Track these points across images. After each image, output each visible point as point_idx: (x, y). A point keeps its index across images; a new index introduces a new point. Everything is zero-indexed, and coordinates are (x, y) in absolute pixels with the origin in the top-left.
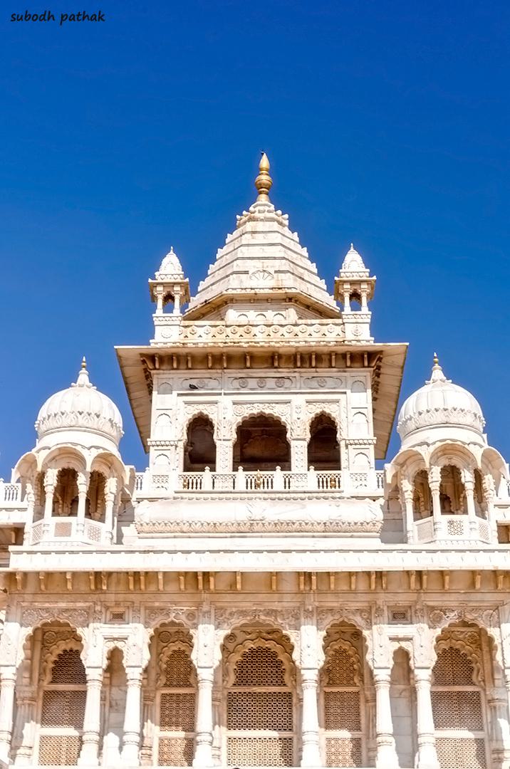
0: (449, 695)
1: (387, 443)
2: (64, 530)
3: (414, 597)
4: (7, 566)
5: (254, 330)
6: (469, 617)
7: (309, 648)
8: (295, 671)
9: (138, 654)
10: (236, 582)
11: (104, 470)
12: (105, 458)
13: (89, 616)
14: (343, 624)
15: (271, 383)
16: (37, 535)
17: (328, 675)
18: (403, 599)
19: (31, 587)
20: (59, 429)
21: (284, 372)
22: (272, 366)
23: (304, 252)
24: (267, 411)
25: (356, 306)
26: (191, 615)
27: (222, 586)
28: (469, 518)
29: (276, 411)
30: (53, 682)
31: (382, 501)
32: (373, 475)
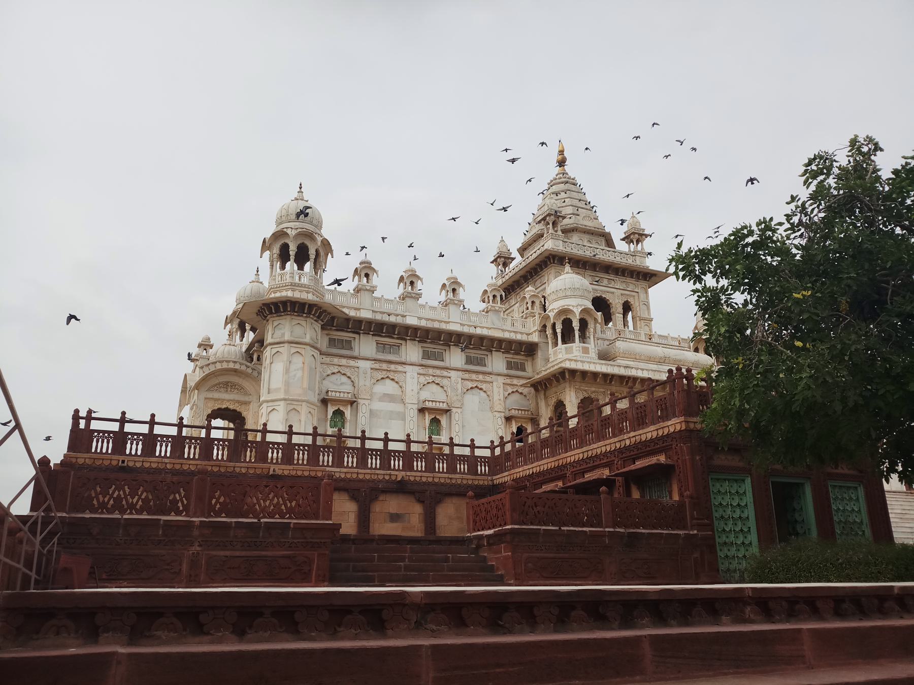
15: (605, 282)
21: (612, 277)
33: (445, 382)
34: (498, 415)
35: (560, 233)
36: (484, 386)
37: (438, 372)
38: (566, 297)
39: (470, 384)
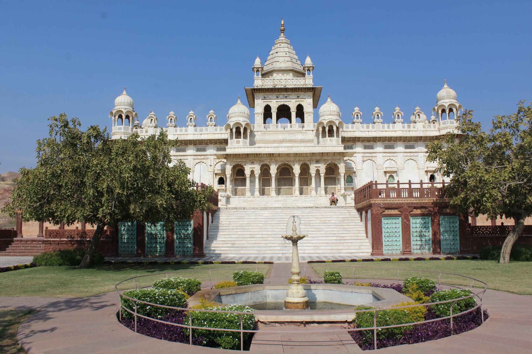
0: (329, 177)
1: (316, 117)
3: (321, 157)
4: (225, 150)
5: (282, 81)
6: (333, 162)
7: (297, 169)
10: (279, 155)
11: (247, 127)
12: (247, 124)
13: (246, 163)
14: (304, 164)
16: (231, 143)
17: (301, 174)
18: (318, 158)
19: (232, 157)
20: (235, 117)
21: (289, 93)
22: (286, 92)
23: (294, 52)
25: (309, 74)
28: (335, 138)
30: (237, 176)
31: (315, 132)
32: (312, 124)
35: (260, 76)
36: (204, 161)
38: (238, 116)
39: (198, 161)
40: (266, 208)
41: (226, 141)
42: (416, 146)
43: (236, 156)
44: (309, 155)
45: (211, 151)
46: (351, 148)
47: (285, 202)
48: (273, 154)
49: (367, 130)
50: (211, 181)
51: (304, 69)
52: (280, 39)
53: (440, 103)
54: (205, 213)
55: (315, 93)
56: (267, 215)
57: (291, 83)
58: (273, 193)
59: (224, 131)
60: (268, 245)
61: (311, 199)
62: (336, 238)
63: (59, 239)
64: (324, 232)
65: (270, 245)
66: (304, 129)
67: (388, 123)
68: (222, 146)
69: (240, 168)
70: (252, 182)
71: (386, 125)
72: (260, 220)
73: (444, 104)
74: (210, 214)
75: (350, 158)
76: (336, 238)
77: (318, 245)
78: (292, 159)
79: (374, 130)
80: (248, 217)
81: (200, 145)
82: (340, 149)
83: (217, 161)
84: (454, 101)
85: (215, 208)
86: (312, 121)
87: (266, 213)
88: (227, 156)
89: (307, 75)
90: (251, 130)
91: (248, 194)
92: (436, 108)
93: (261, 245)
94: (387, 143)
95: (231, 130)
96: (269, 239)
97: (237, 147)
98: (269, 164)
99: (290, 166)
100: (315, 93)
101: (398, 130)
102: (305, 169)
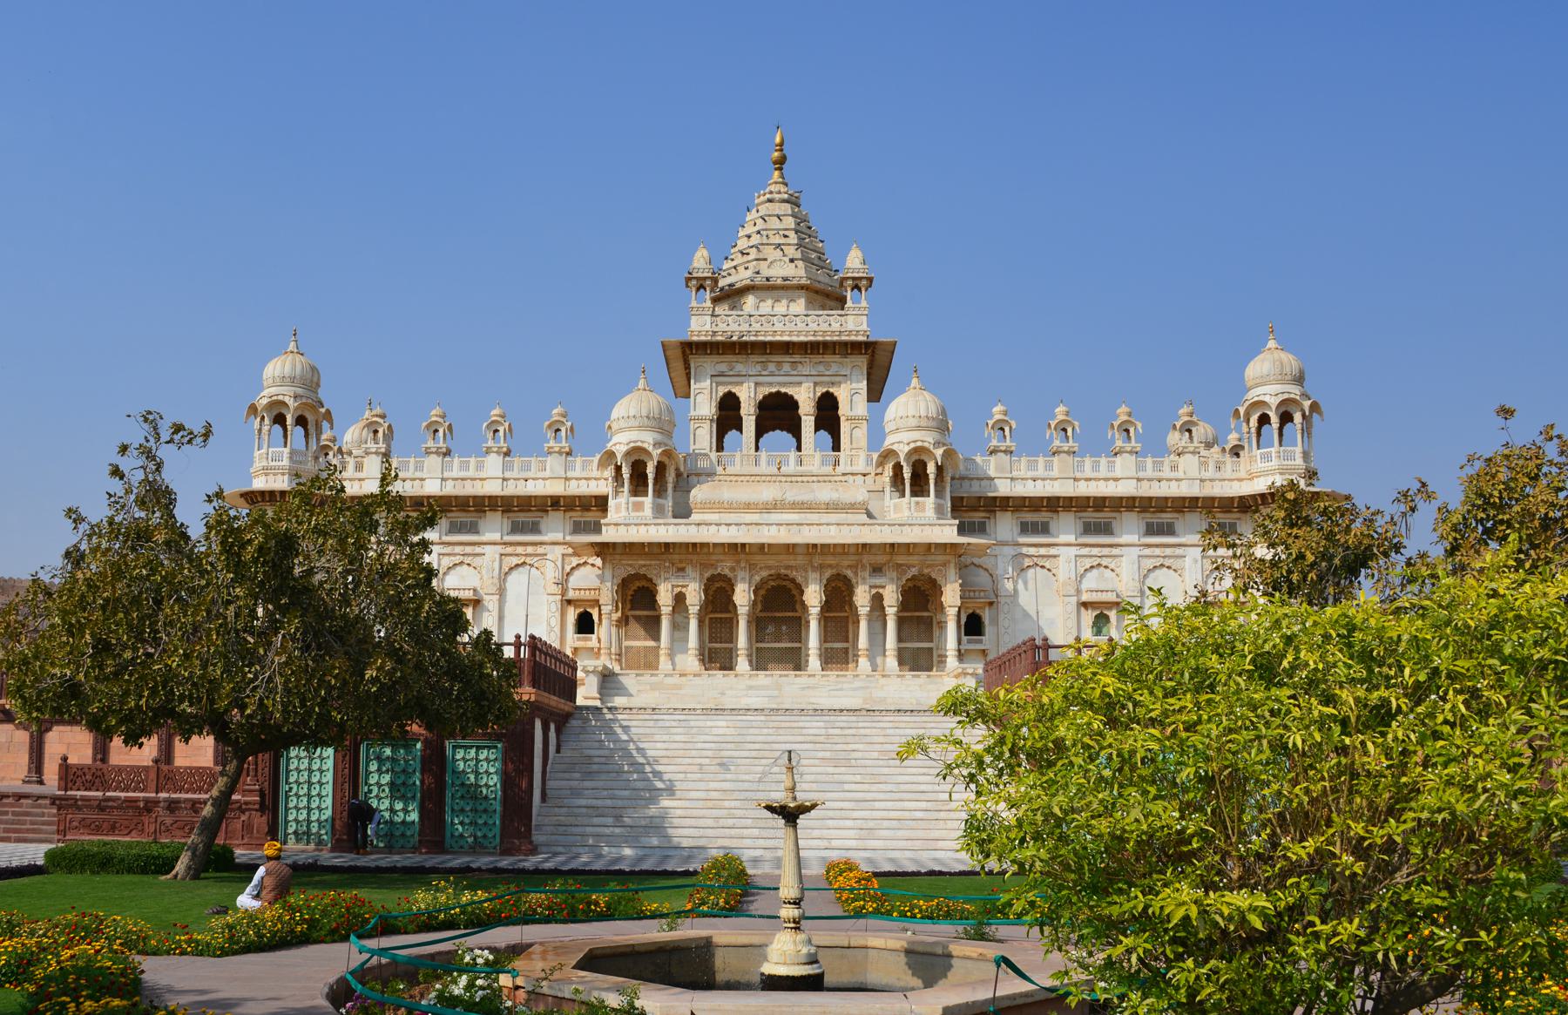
2: (639, 507)
4: (597, 529)
7: (813, 596)
8: (805, 607)
9: (694, 594)
12: (668, 453)
15: (786, 367)
17: (826, 607)
18: (881, 559)
19: (619, 550)
21: (797, 358)
22: (787, 353)
24: (783, 390)
26: (733, 569)
27: (754, 550)
28: (930, 501)
29: (790, 391)
32: (862, 455)
33: (477, 561)
34: (552, 598)
35: (709, 304)
37: (468, 549)
39: (515, 561)
40: (720, 710)
41: (601, 503)
42: (1178, 526)
43: (630, 548)
44: (852, 550)
45: (555, 530)
46: (980, 529)
47: (776, 693)
48: (743, 545)
49: (1030, 474)
50: (555, 622)
51: (841, 285)
52: (772, 188)
53: (1253, 396)
54: (538, 724)
55: (875, 360)
56: (721, 731)
57: (801, 326)
58: (742, 664)
59: (596, 474)
60: (722, 822)
61: (857, 684)
62: (924, 805)
63: (99, 794)
64: (890, 787)
65: (730, 822)
66: (840, 470)
67: (1096, 454)
68: (590, 516)
69: (644, 583)
70: (679, 627)
71: (1088, 462)
72: (699, 746)
73: (1267, 399)
74: (552, 727)
75: (976, 561)
76: (924, 805)
77: (871, 824)
78: (801, 560)
79: (1055, 473)
80: (665, 738)
81: (524, 512)
82: (947, 533)
83: (575, 561)
84: (1295, 391)
85: (564, 705)
86: (864, 443)
87: (721, 725)
88: (605, 550)
89: (849, 304)
90: (677, 469)
91: (664, 663)
92: (1242, 410)
93: (701, 822)
94: (1091, 516)
95: (618, 469)
96: (727, 804)
97: (633, 520)
98: (730, 575)
99: (793, 581)
100: (875, 360)
101: (1119, 476)
102: (838, 596)
